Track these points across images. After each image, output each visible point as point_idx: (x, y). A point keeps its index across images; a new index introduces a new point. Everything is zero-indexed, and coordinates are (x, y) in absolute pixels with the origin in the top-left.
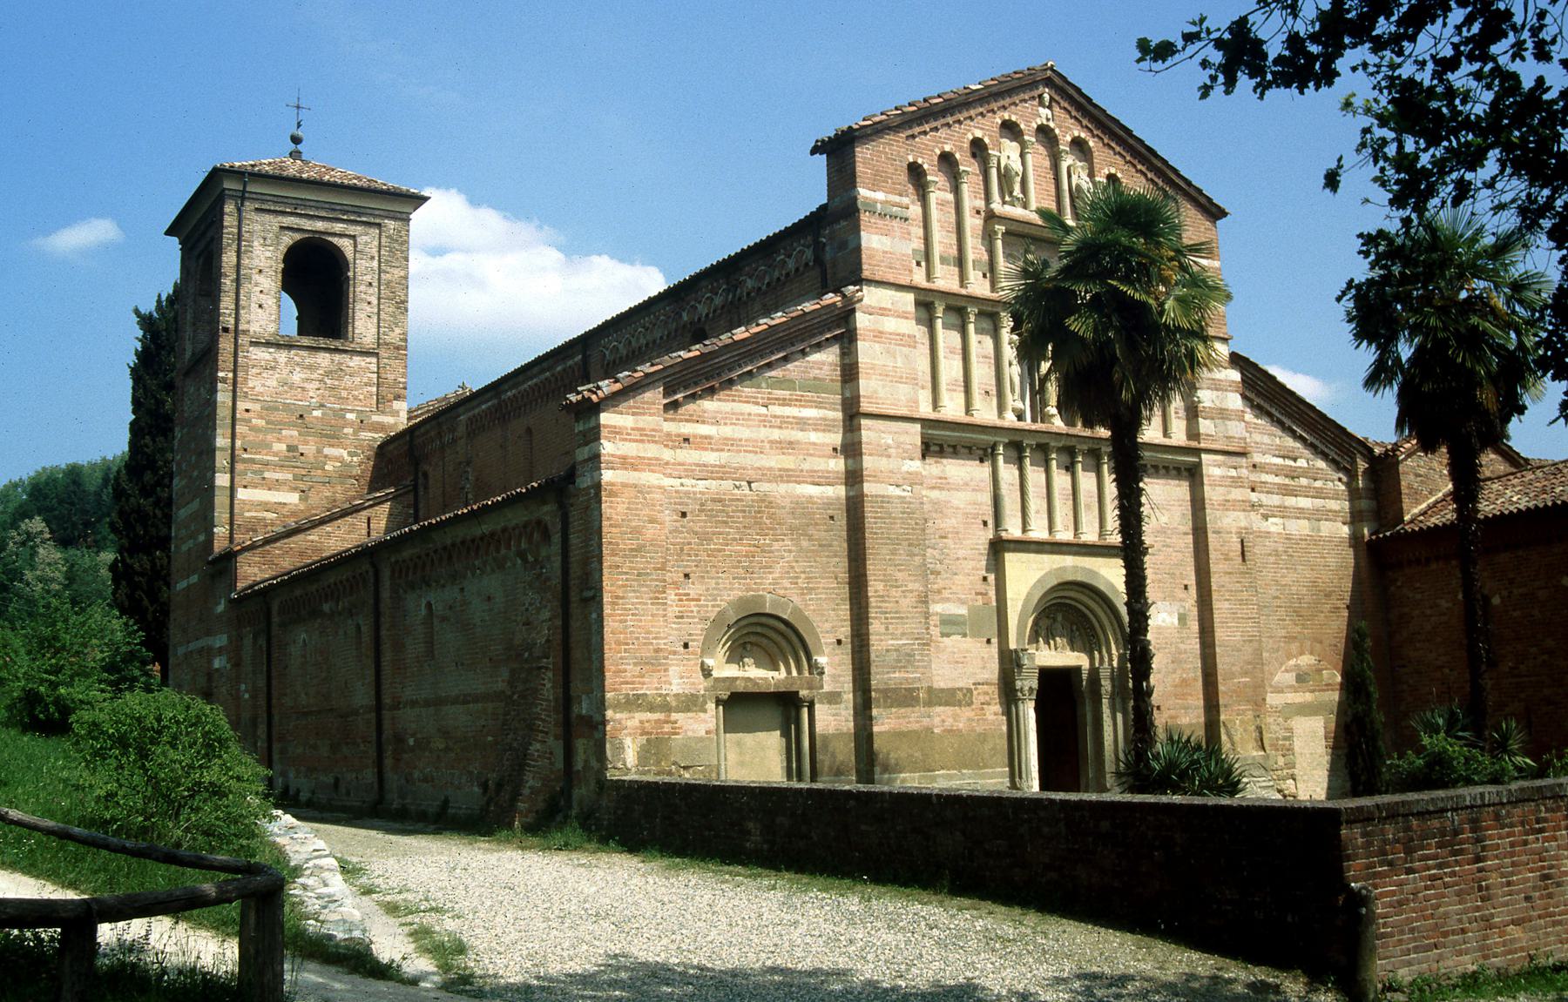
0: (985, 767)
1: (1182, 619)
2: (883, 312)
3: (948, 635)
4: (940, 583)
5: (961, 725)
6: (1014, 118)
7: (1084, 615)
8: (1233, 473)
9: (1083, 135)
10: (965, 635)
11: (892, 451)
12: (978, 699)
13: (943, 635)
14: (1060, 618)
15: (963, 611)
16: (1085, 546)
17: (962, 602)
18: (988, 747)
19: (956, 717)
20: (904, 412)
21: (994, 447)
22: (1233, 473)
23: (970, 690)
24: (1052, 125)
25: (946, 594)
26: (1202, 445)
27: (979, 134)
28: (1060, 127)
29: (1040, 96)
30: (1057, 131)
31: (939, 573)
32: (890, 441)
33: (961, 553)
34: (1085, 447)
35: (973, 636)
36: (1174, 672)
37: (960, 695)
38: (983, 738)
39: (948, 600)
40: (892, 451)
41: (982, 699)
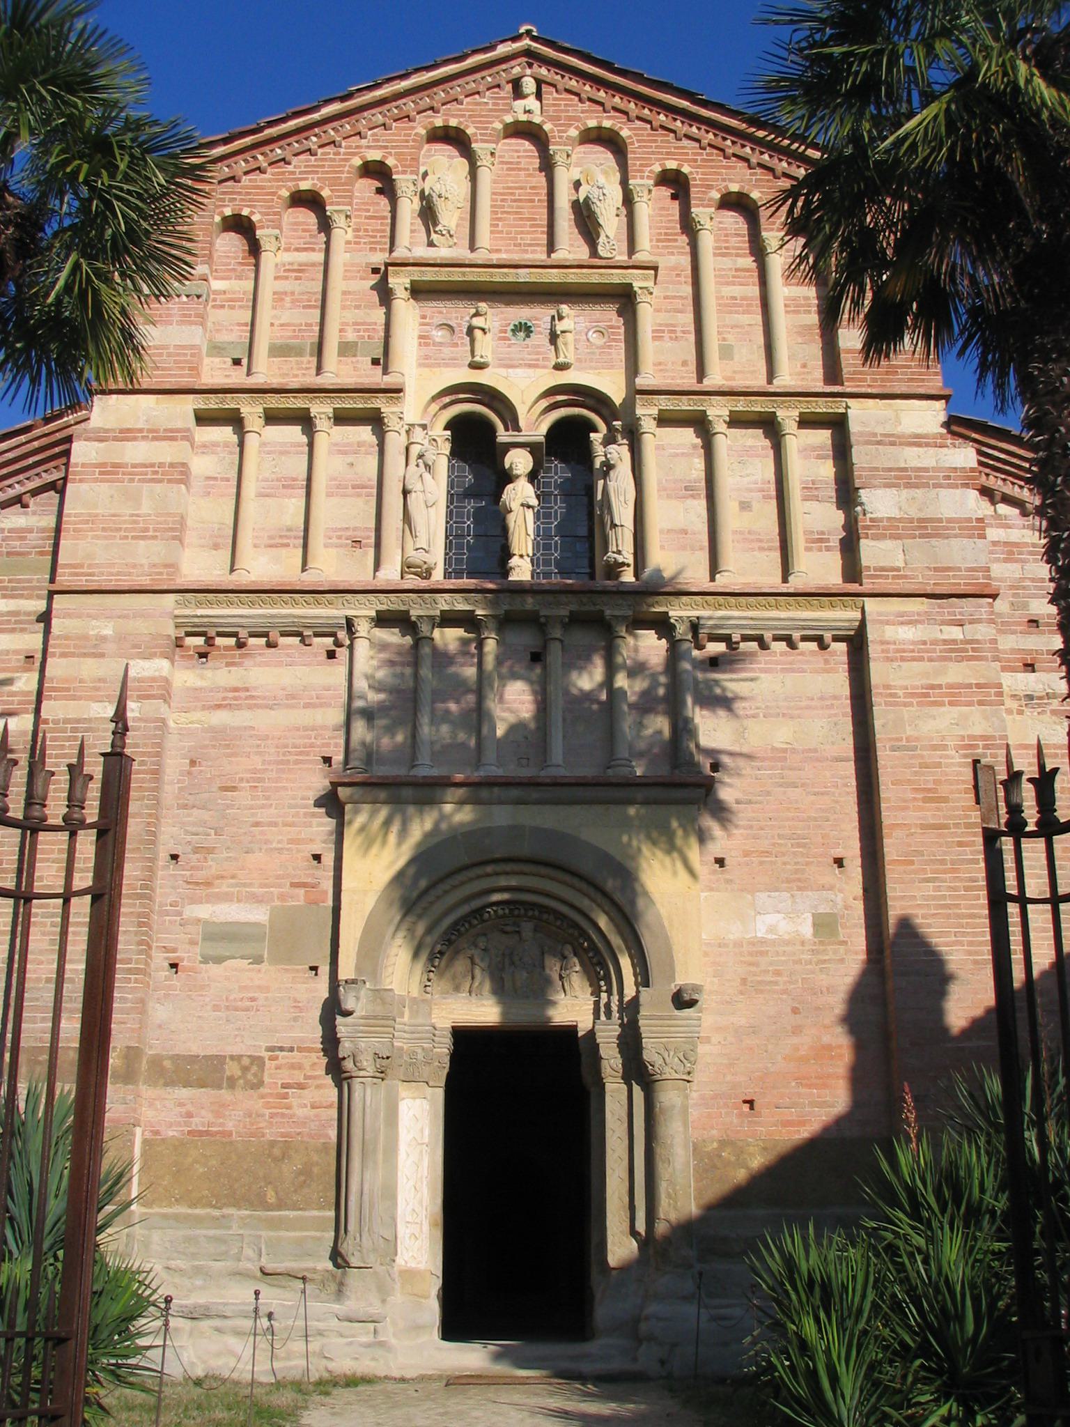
0: (280, 1205)
1: (825, 925)
2: (127, 435)
3: (219, 960)
4: (213, 866)
5: (230, 1126)
6: (453, 123)
7: (576, 926)
8: (955, 633)
9: (607, 124)
10: (258, 960)
11: (110, 647)
12: (273, 1076)
13: (206, 960)
14: (527, 928)
15: (259, 915)
16: (556, 784)
17: (257, 900)
18: (288, 1170)
19: (220, 1109)
20: (145, 582)
21: (350, 624)
22: (955, 633)
23: (258, 1061)
24: (537, 119)
25: (224, 887)
26: (867, 586)
27: (374, 155)
28: (551, 119)
29: (516, 84)
30: (547, 127)
31: (210, 850)
32: (108, 631)
33: (263, 816)
34: (564, 612)
35: (275, 960)
36: (797, 1030)
37: (232, 1069)
38: (282, 1150)
39: (226, 898)
40: (110, 647)
41: (286, 1076)
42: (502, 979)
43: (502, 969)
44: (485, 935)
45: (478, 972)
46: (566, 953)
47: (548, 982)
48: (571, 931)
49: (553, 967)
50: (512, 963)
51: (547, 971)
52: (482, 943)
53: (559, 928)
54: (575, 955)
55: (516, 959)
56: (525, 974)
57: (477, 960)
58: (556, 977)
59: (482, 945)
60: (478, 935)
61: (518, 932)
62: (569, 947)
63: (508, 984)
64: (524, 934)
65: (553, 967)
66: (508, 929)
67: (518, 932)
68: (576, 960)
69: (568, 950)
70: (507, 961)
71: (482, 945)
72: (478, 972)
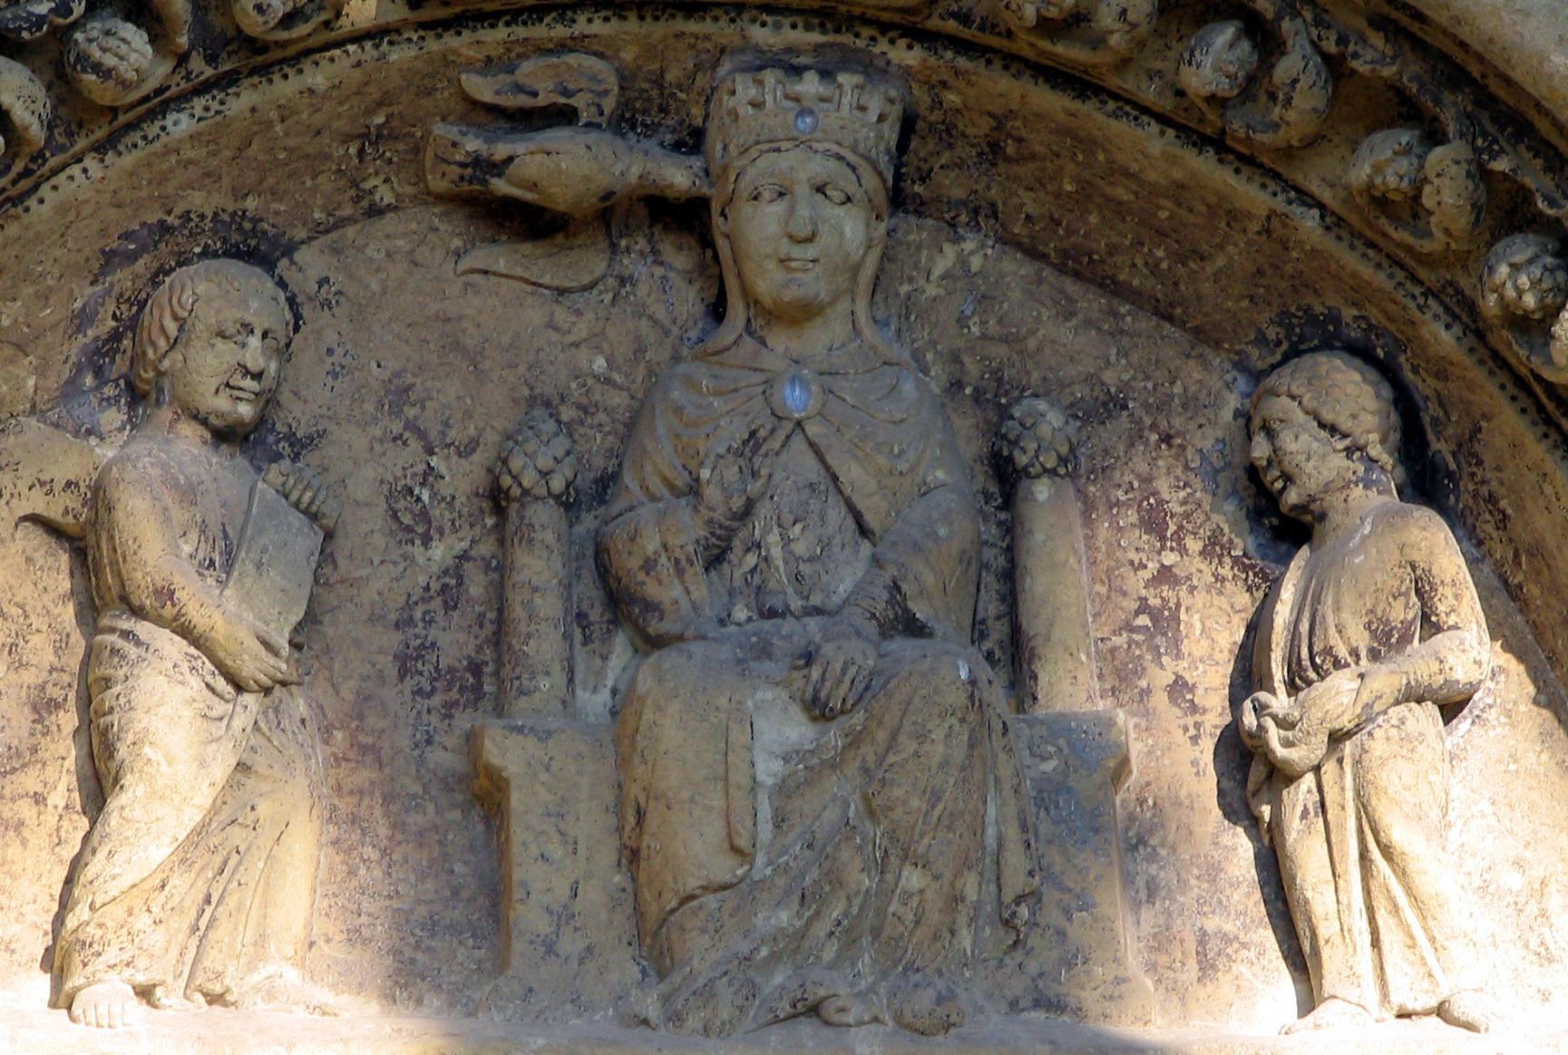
42: (485, 797)
43: (486, 680)
44: (256, 248)
45: (175, 722)
46: (1313, 463)
47: (1081, 816)
48: (1381, 160)
49: (1149, 636)
50: (617, 605)
51: (1071, 687)
52: (217, 325)
53: (1197, 127)
54: (1425, 481)
55: (656, 536)
56: (781, 730)
57: (153, 545)
58: (1174, 759)
59: (211, 372)
60: (165, 243)
61: (687, 218)
62: (1354, 395)
63: (559, 863)
64: (759, 228)
65: (1149, 636)
66: (565, 165)
67: (687, 218)
68: (1437, 545)
69: (1331, 427)
70: (541, 568)
71: (211, 372)
72: (175, 722)
